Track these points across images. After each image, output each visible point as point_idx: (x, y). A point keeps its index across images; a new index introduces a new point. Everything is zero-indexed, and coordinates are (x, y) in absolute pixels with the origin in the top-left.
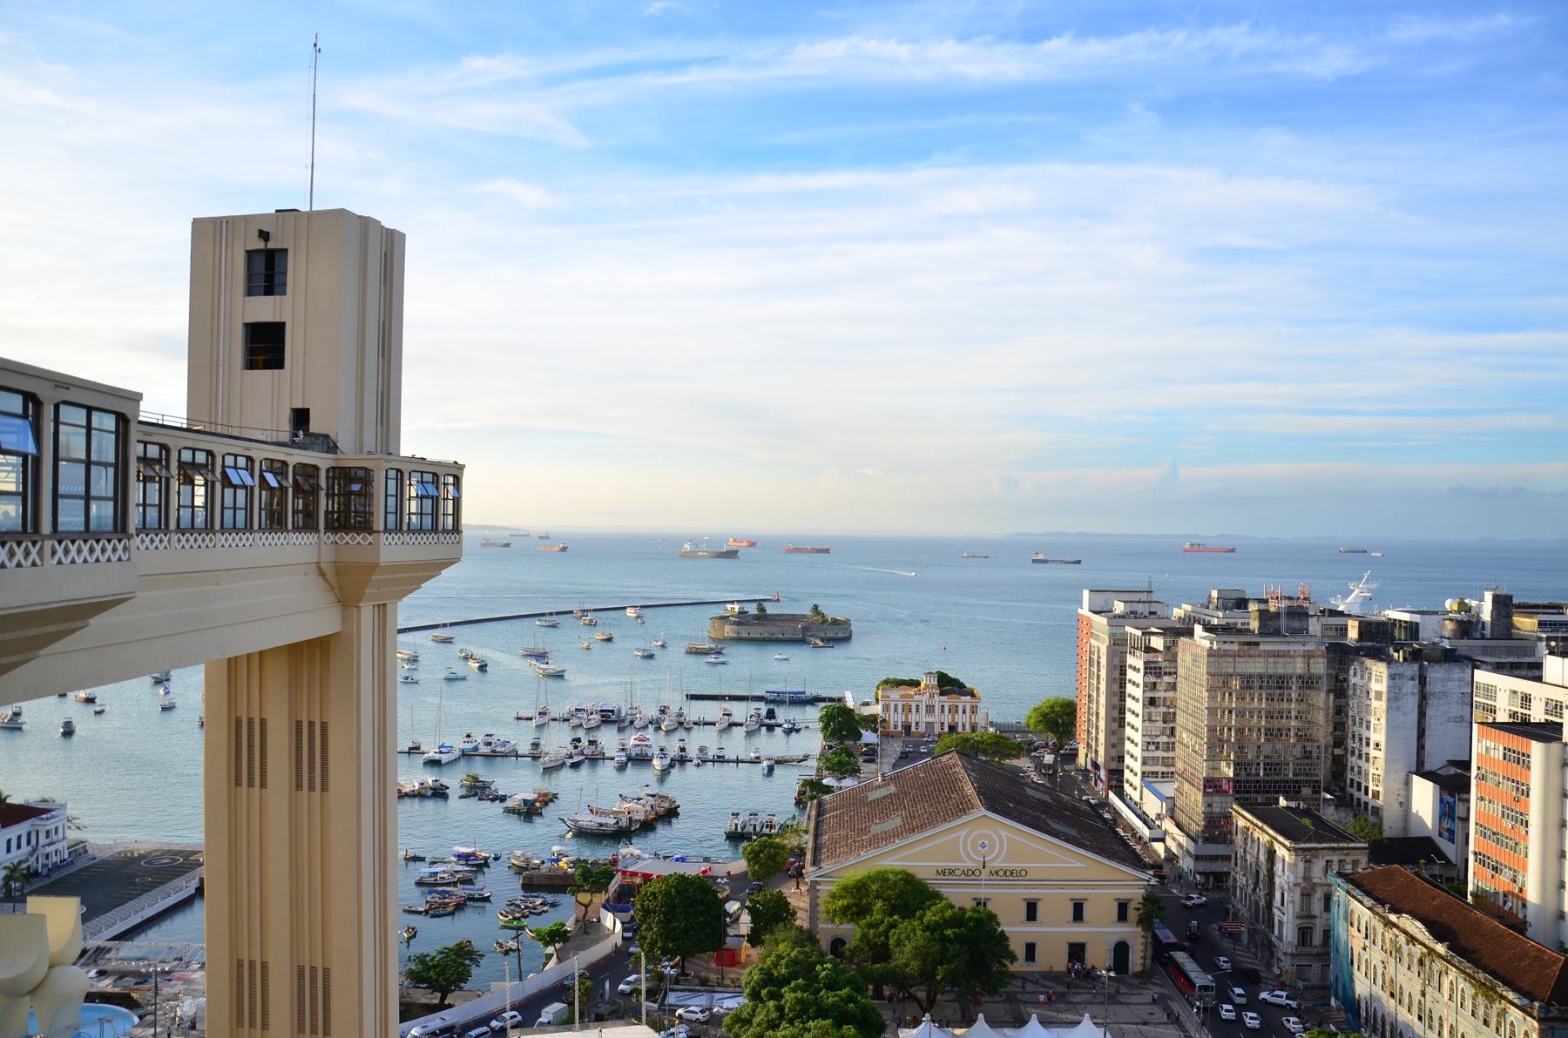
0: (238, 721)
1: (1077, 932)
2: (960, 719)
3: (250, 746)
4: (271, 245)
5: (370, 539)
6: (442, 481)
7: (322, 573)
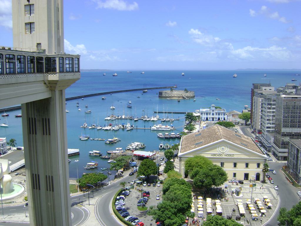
0: (29, 119)
1: (247, 171)
2: (221, 116)
4: (30, 3)
6: (75, 60)
7: (45, 84)
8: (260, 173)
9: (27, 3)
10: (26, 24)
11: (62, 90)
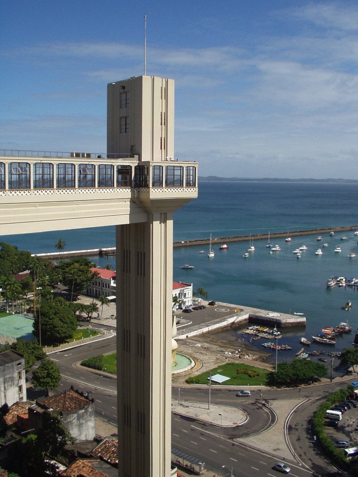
5: (148, 190)
9: (122, 91)
10: (121, 118)
11: (166, 213)
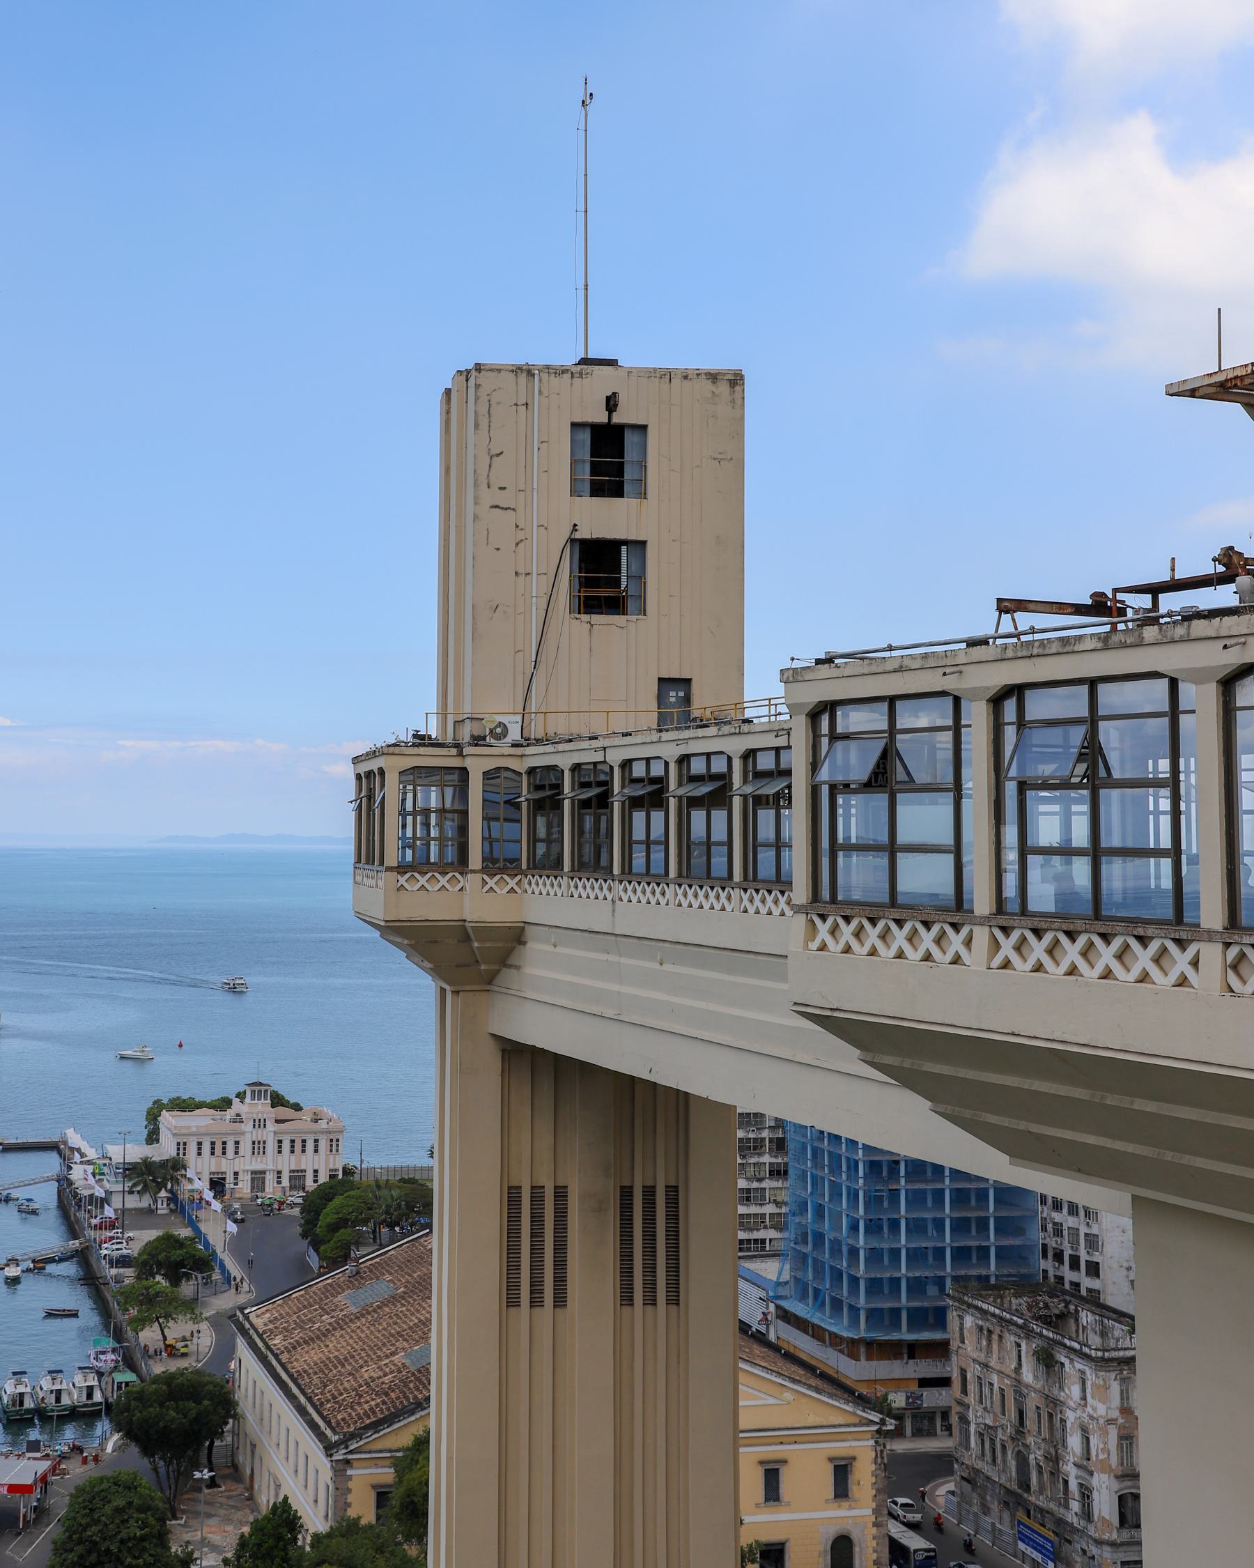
3: (537, 1236)
8: (855, 1536)
